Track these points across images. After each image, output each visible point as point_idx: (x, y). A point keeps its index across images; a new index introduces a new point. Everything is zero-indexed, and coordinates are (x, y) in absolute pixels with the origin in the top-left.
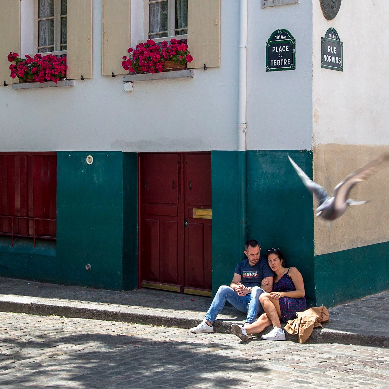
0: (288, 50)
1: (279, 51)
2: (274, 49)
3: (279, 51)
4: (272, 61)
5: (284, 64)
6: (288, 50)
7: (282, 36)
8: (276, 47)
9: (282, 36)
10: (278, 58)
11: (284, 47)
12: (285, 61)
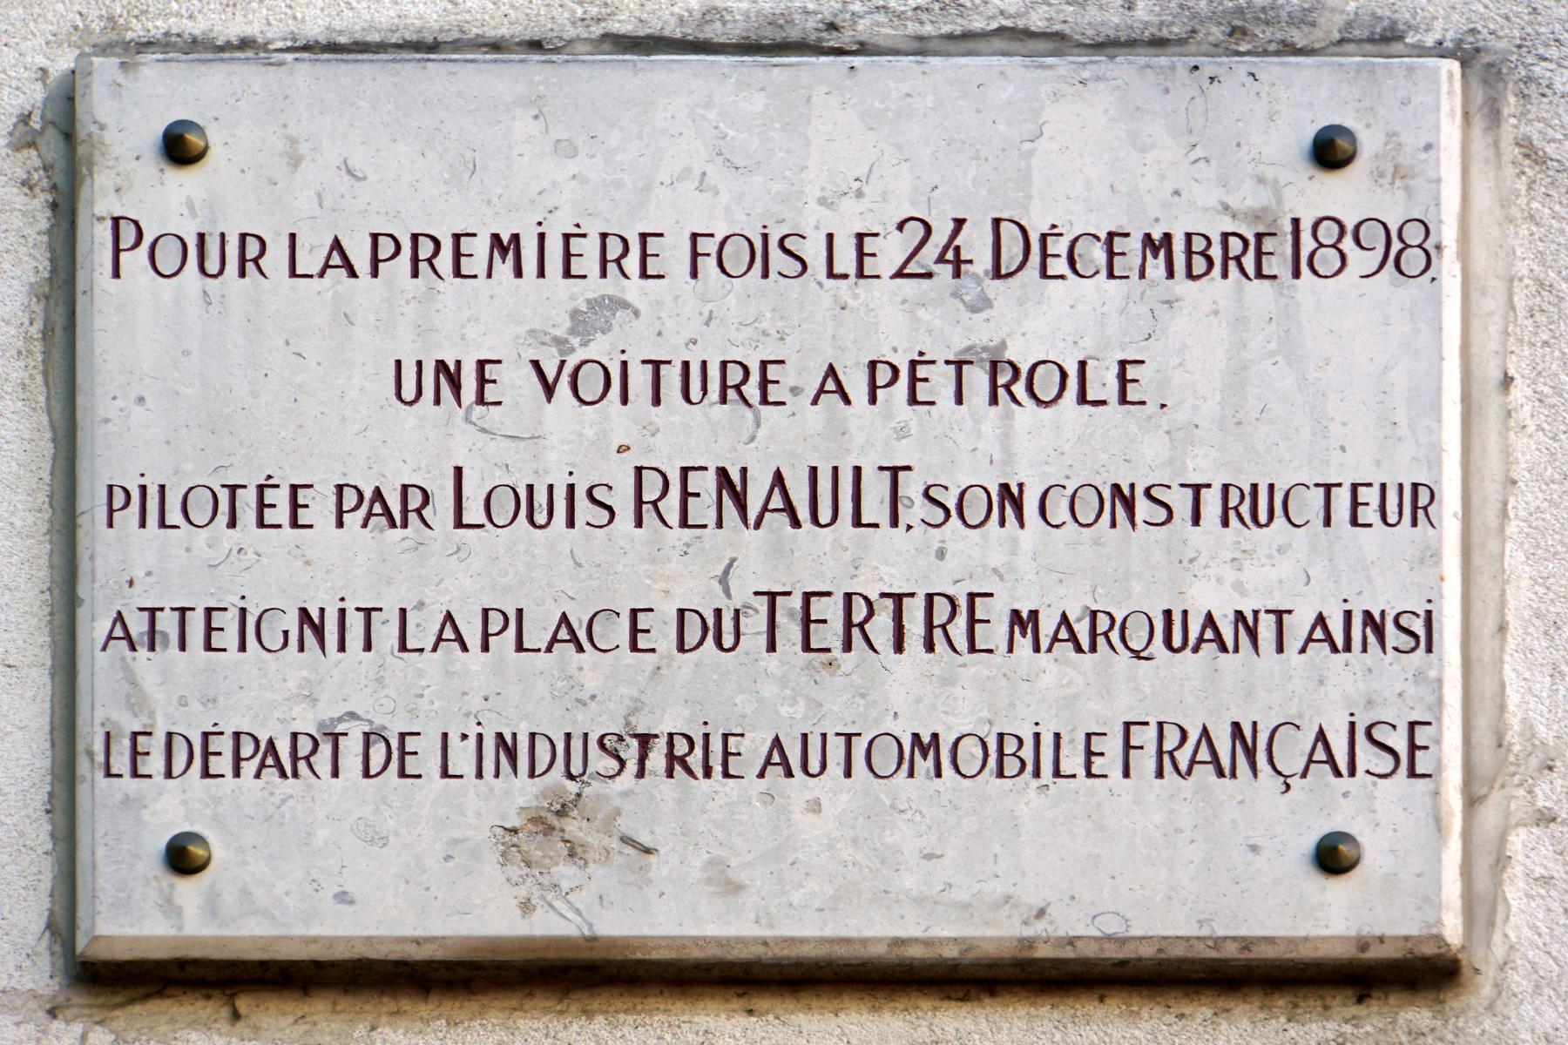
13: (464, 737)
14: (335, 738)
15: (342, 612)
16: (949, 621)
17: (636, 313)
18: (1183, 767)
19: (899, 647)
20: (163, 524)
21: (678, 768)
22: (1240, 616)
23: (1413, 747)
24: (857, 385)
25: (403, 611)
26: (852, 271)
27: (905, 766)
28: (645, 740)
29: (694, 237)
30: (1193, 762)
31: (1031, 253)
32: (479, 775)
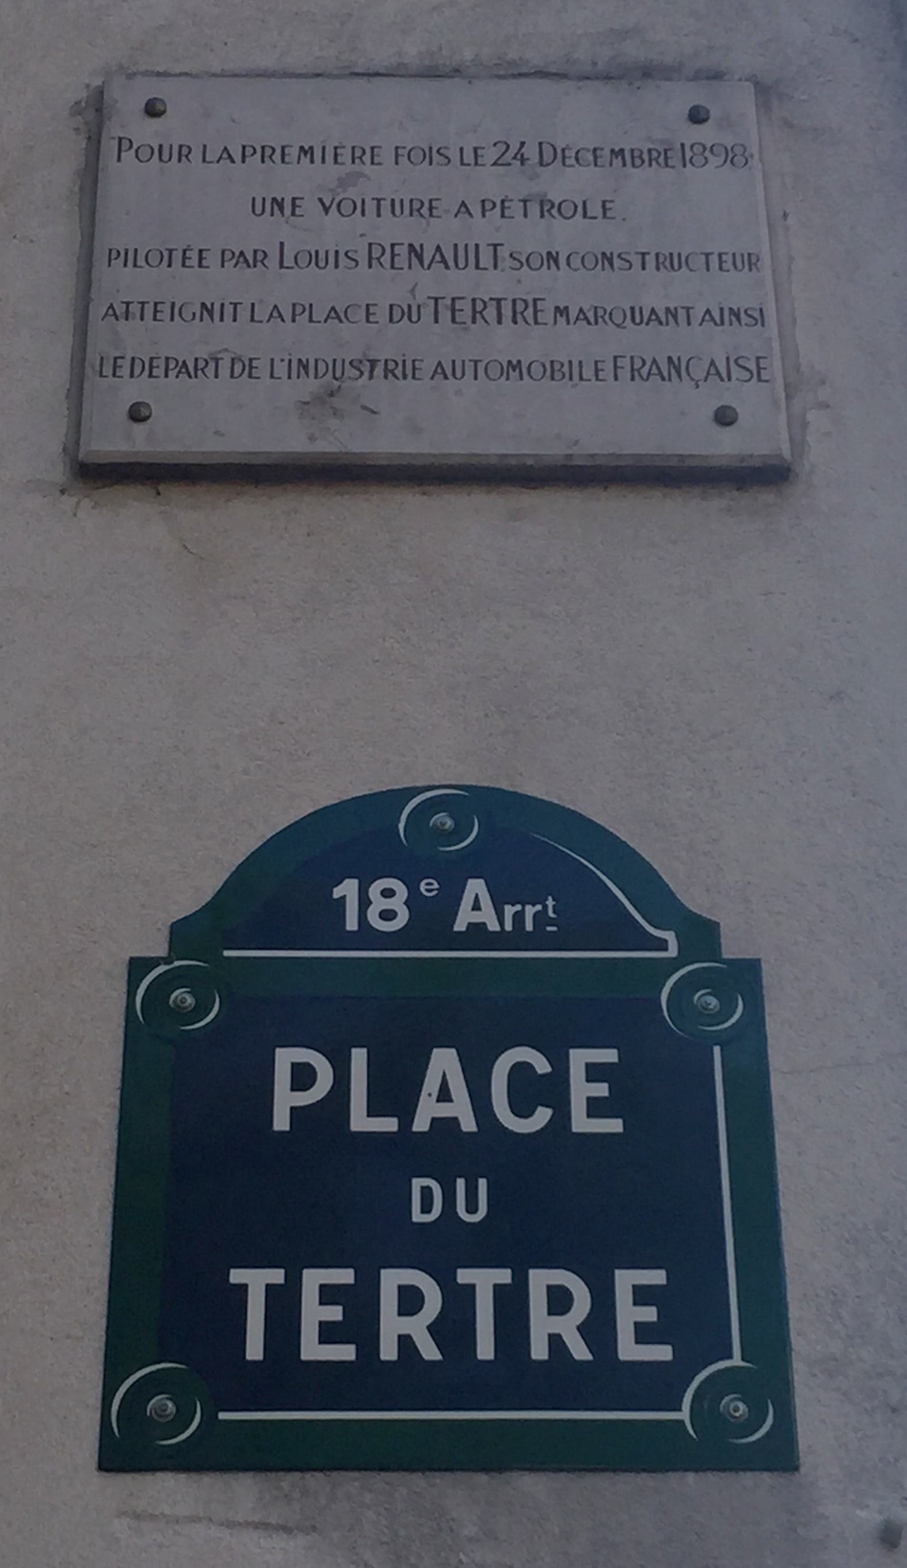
0: (614, 1126)
1: (421, 1124)
2: (294, 1083)
3: (421, 1124)
4: (256, 1281)
5: (539, 1351)
6: (614, 1126)
7: (475, 887)
8: (359, 1057)
9: (475, 887)
10: (370, 1236)
11: (520, 1072)
13: (282, 360)
14: (217, 361)
15: (223, 305)
16: (524, 311)
17: (369, 179)
18: (645, 376)
19: (499, 322)
20: (135, 265)
21: (390, 375)
22: (668, 310)
23: (759, 369)
24: (476, 209)
25: (253, 305)
26: (473, 162)
27: (505, 374)
28: (373, 363)
29: (397, 148)
30: (649, 374)
32: (289, 377)
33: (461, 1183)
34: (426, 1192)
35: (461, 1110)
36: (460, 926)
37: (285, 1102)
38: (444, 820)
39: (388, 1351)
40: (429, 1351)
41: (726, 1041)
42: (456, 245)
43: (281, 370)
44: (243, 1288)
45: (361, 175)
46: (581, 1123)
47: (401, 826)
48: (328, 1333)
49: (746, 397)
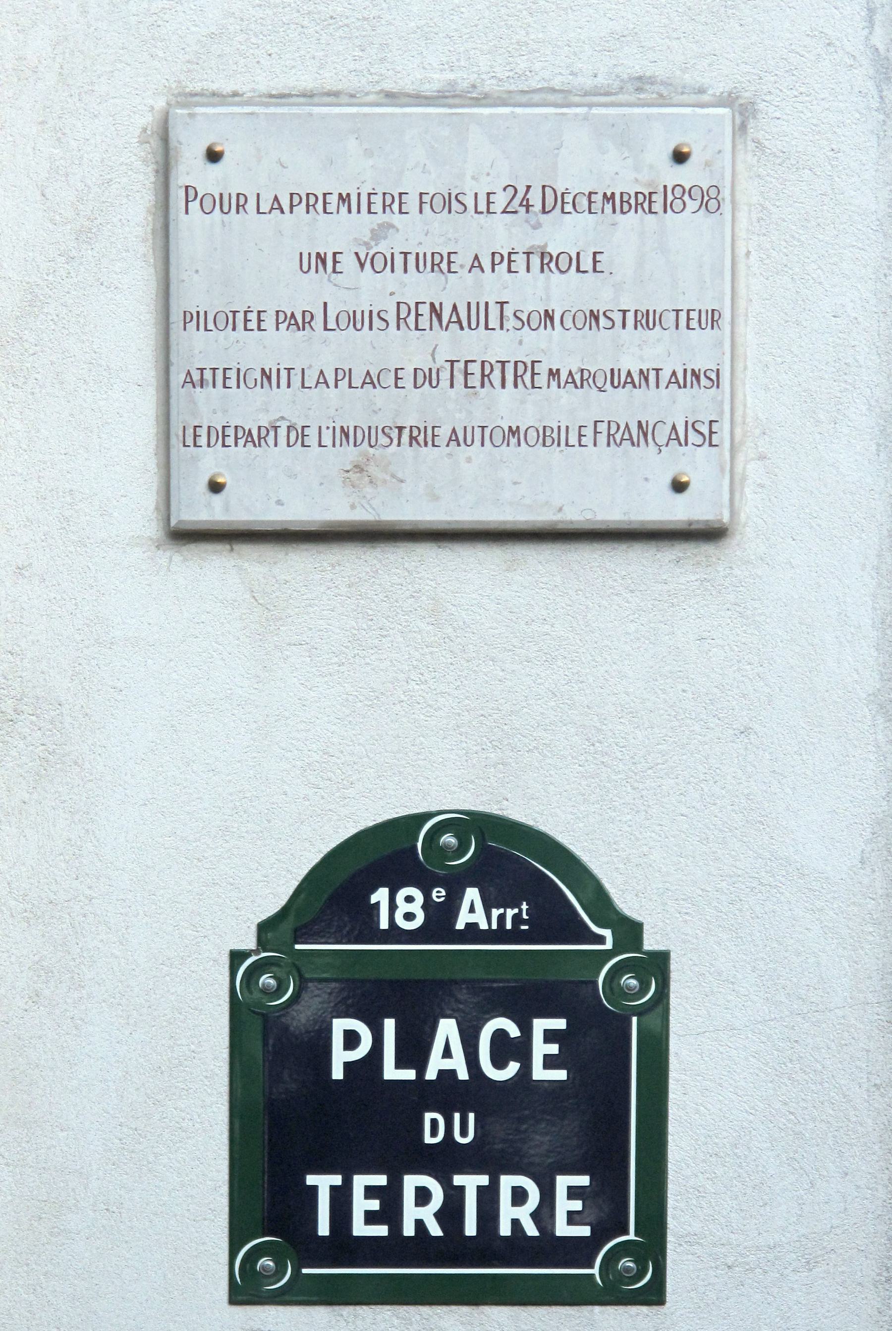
0: (561, 1075)
1: (431, 1074)
2: (348, 1045)
3: (431, 1074)
4: (324, 1183)
5: (505, 1230)
6: (561, 1075)
7: (472, 894)
8: (390, 1025)
9: (472, 894)
11: (500, 1036)
12: (519, 1197)
13: (328, 428)
14: (276, 428)
15: (278, 370)
16: (522, 373)
17: (398, 230)
18: (618, 441)
19: (503, 386)
20: (206, 330)
21: (414, 442)
22: (641, 371)
23: (711, 433)
24: (486, 263)
25: (303, 369)
26: (485, 210)
27: (506, 441)
28: (400, 429)
29: (421, 194)
30: (622, 439)
31: (556, 202)
32: (334, 446)
33: (457, 1116)
34: (434, 1122)
35: (459, 1065)
36: (460, 925)
37: (340, 1059)
38: (448, 839)
39: (409, 1230)
40: (435, 1230)
41: (641, 1012)
42: (469, 303)
43: (327, 439)
44: (315, 1188)
45: (391, 226)
46: (539, 1073)
47: (419, 845)
48: (371, 1218)
49: (696, 464)
